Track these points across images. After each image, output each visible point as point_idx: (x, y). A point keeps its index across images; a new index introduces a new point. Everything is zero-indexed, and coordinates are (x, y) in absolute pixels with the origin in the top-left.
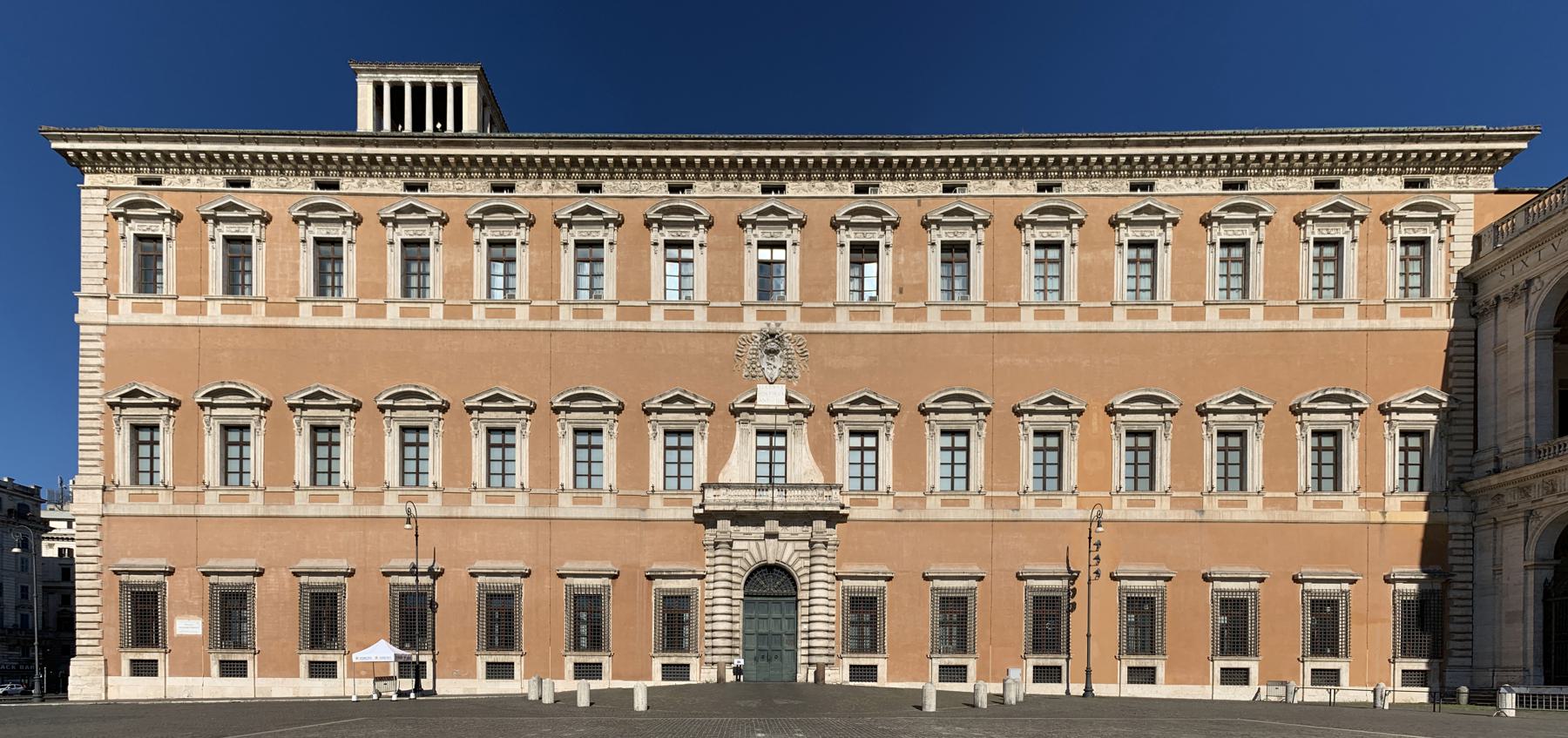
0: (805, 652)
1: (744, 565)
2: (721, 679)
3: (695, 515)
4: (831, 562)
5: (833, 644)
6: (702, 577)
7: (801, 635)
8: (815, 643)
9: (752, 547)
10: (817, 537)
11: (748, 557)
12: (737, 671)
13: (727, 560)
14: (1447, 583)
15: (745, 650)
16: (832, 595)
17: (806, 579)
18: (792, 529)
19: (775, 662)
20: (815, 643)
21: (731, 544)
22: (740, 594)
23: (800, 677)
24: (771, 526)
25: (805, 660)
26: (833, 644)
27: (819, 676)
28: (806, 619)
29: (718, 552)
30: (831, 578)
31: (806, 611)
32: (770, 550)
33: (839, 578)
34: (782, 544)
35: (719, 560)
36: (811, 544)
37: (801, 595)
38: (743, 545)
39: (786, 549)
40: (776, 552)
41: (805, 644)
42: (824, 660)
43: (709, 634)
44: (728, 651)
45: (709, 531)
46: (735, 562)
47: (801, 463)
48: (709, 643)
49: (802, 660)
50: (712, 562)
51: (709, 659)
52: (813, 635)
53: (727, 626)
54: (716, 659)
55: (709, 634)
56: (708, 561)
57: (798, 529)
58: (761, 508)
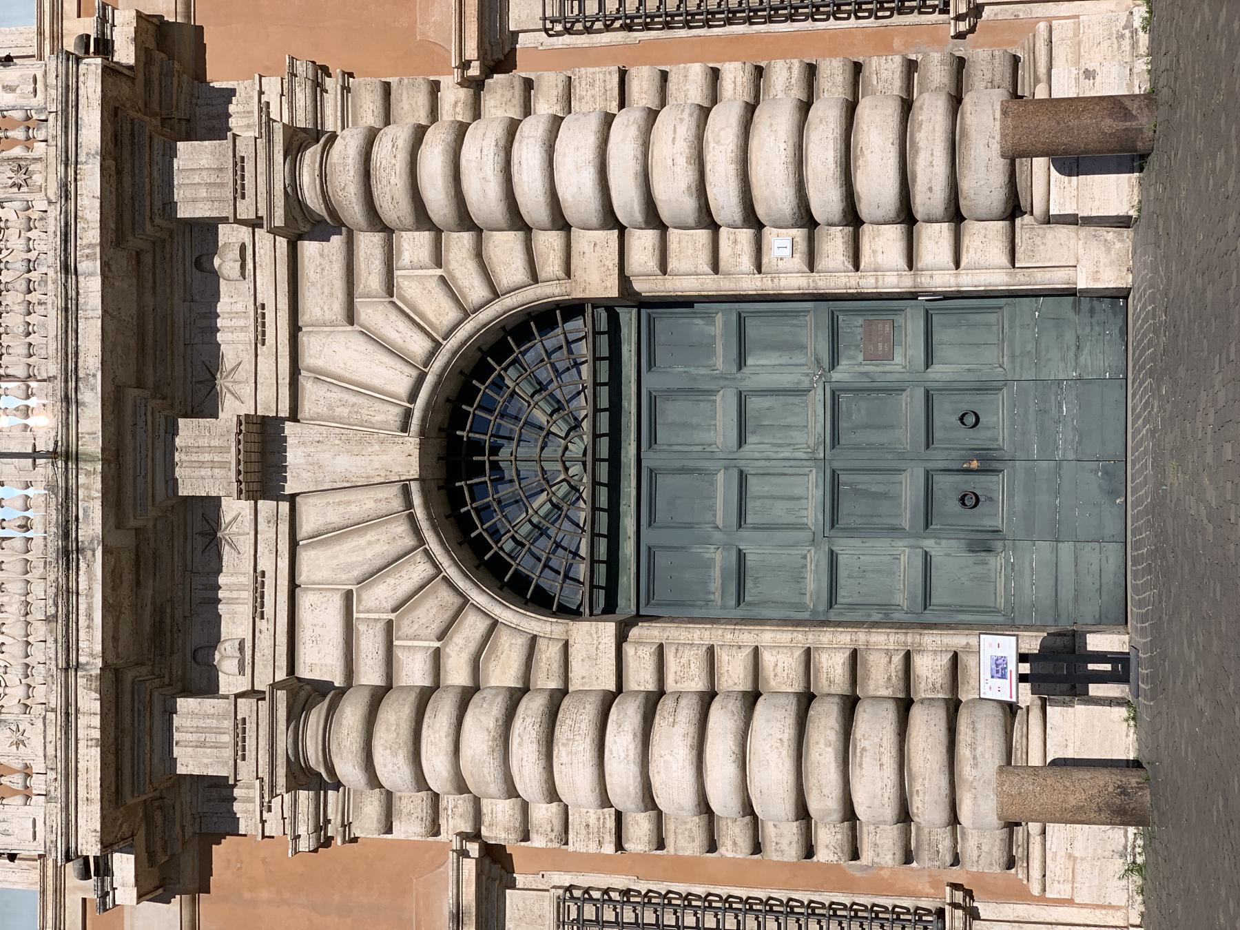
0: (935, 240)
1: (431, 613)
2: (1124, 794)
3: (155, 886)
4: (412, 106)
5: (885, 72)
6: (496, 866)
7: (835, 273)
8: (877, 184)
9: (333, 563)
10: (264, 192)
12: (1060, 671)
13: (395, 716)
15: (926, 612)
16: (596, 87)
17: (505, 250)
18: (233, 337)
19: (999, 423)
20: (877, 184)
21: (305, 696)
22: (592, 640)
23: (1099, 264)
24: (204, 458)
25: (984, 241)
26: (885, 72)
27: (1097, 140)
28: (736, 243)
30: (500, 98)
31: (689, 247)
32: (344, 463)
33: (499, 55)
34: (314, 396)
35: (392, 766)
36: (323, 225)
37: (596, 278)
39: (339, 367)
40: (355, 432)
41: (884, 244)
42: (985, 116)
43: (829, 839)
44: (926, 727)
45: (246, 810)
46: (414, 672)
48: (880, 845)
49: (985, 261)
50: (412, 806)
51: (982, 847)
52: (826, 199)
53: (772, 728)
54: (980, 808)
55: (829, 839)
56: (408, 828)
57: (233, 305)
58: (91, 526)
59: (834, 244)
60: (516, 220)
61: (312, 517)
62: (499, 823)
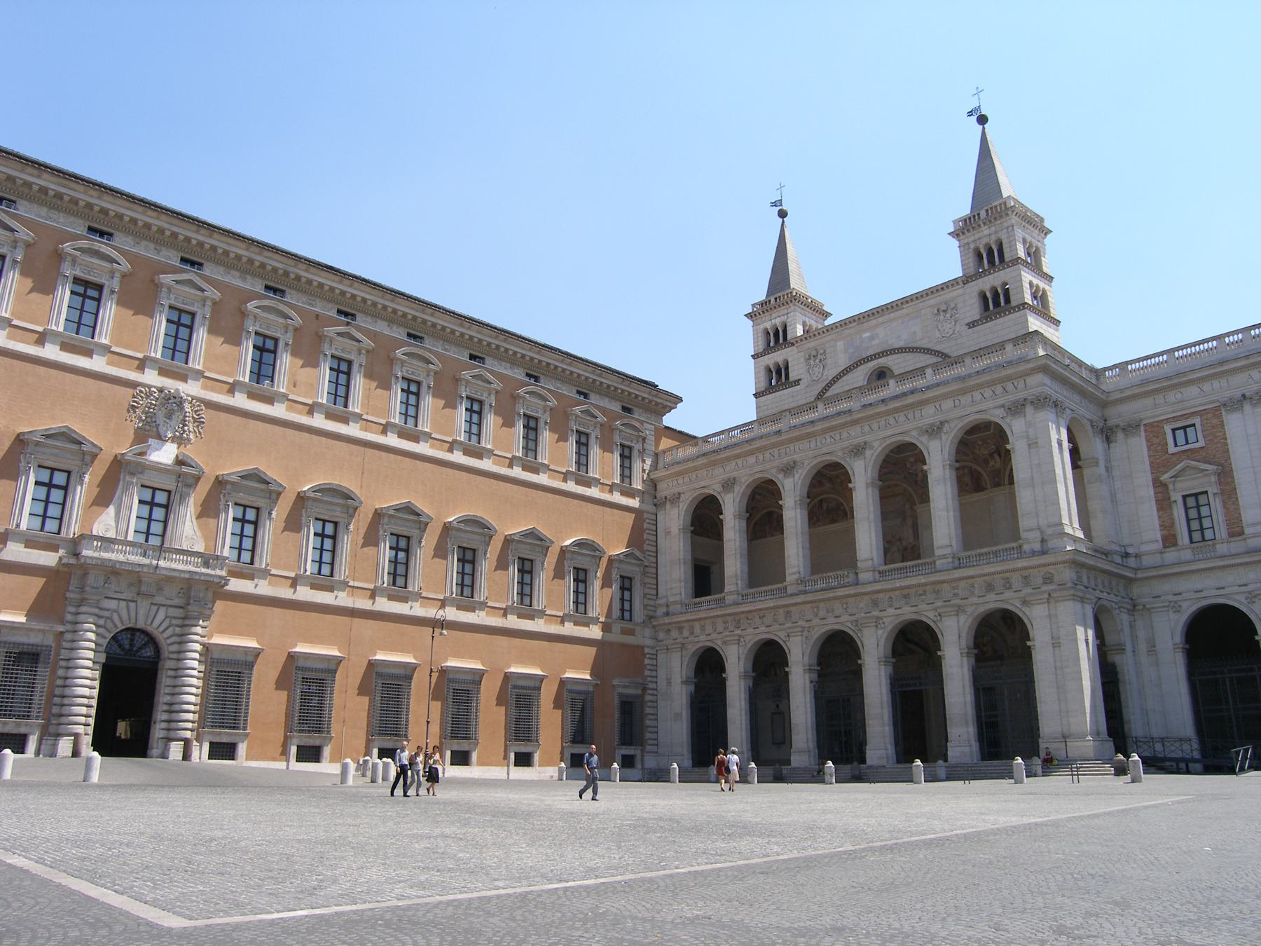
0: (164, 725)
1: (109, 625)
11: (115, 616)
14: (644, 689)
29: (83, 609)
32: (142, 612)
38: (112, 604)
41: (165, 716)
47: (188, 529)
56: (69, 617)
59: (165, 708)
60: (179, 652)
61: (132, 605)
62: (68, 636)
